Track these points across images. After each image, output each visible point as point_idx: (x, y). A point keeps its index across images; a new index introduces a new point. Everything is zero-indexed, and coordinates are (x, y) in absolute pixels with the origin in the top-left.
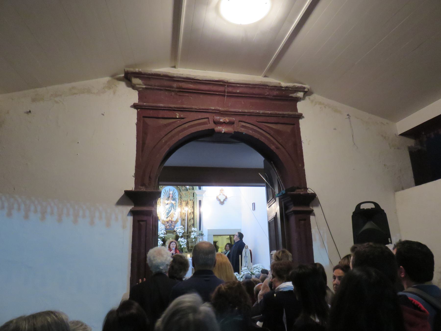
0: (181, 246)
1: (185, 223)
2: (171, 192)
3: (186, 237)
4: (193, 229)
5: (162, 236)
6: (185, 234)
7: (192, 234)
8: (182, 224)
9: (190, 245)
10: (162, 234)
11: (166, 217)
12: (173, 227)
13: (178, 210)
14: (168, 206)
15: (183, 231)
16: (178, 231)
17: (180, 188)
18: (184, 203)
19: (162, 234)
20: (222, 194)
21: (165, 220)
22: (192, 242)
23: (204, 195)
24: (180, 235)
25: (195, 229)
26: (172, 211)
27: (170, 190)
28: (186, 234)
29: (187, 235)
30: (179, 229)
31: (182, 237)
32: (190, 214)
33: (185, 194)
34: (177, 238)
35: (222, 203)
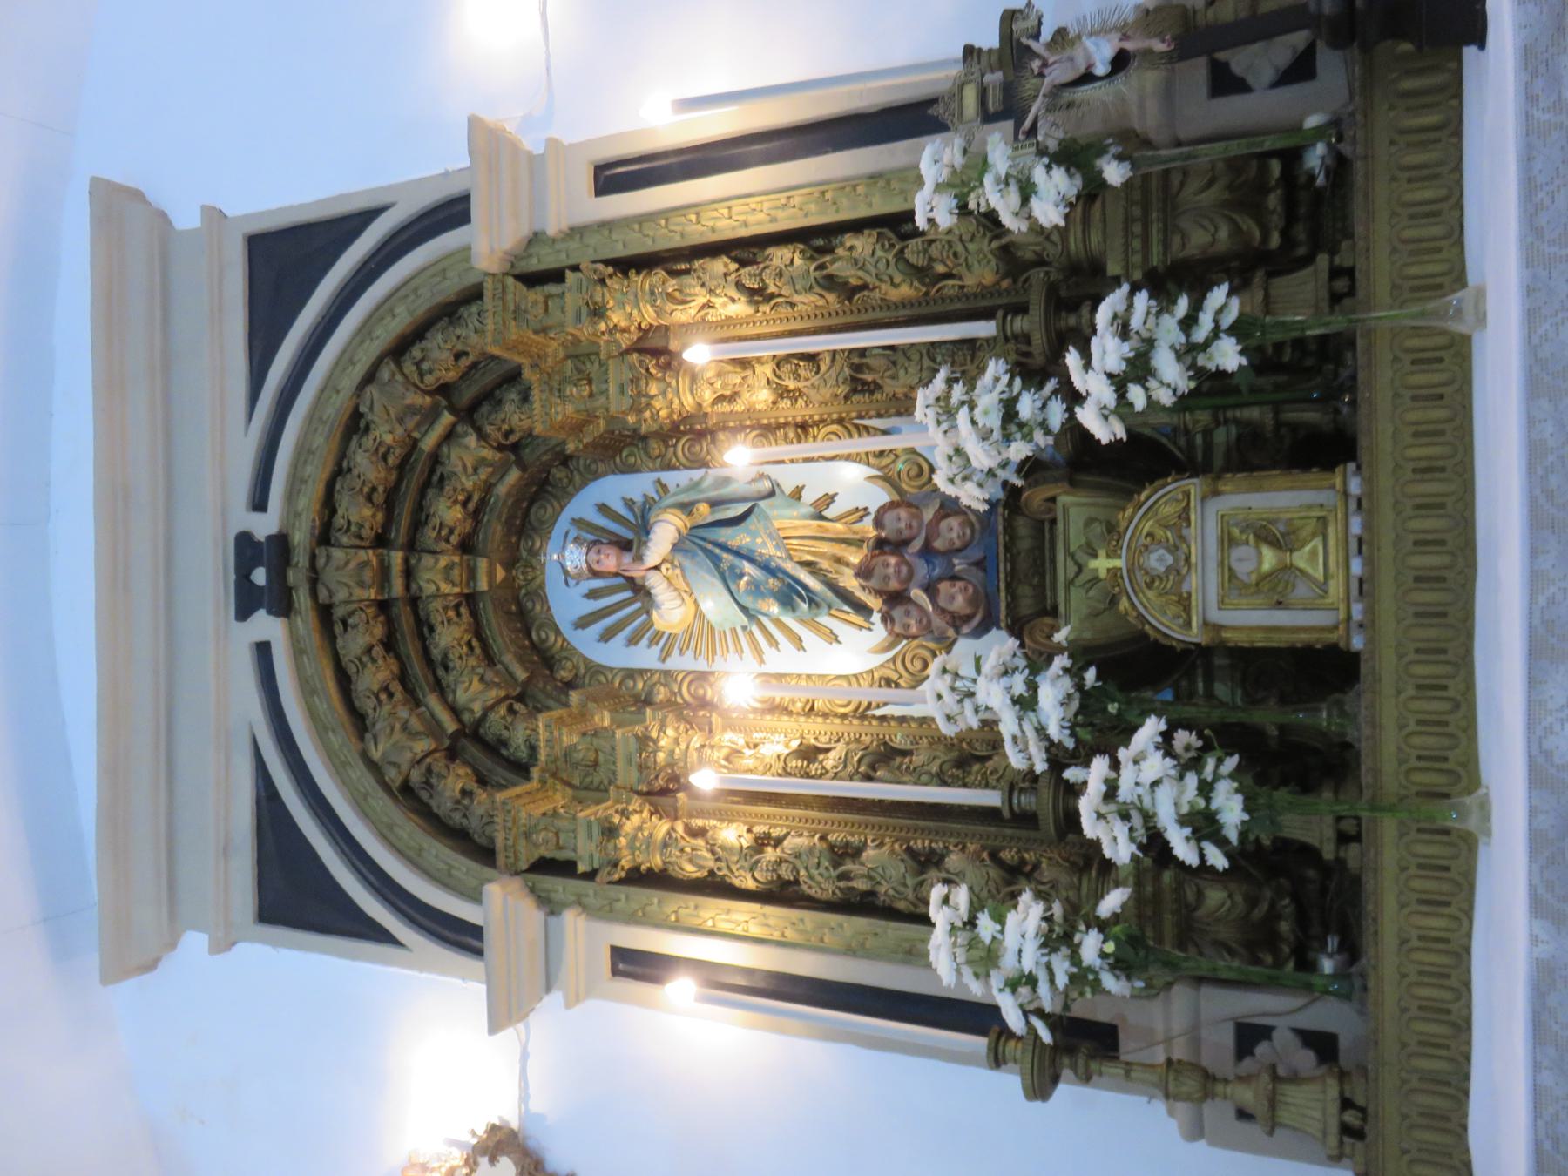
2: (575, 557)
5: (1053, 693)
7: (1003, 203)
8: (905, 407)
10: (1026, 703)
12: (952, 531)
15: (995, 367)
19: (1026, 703)
23: (532, 143)
26: (768, 550)
28: (1029, 323)
30: (964, 441)
32: (758, 295)
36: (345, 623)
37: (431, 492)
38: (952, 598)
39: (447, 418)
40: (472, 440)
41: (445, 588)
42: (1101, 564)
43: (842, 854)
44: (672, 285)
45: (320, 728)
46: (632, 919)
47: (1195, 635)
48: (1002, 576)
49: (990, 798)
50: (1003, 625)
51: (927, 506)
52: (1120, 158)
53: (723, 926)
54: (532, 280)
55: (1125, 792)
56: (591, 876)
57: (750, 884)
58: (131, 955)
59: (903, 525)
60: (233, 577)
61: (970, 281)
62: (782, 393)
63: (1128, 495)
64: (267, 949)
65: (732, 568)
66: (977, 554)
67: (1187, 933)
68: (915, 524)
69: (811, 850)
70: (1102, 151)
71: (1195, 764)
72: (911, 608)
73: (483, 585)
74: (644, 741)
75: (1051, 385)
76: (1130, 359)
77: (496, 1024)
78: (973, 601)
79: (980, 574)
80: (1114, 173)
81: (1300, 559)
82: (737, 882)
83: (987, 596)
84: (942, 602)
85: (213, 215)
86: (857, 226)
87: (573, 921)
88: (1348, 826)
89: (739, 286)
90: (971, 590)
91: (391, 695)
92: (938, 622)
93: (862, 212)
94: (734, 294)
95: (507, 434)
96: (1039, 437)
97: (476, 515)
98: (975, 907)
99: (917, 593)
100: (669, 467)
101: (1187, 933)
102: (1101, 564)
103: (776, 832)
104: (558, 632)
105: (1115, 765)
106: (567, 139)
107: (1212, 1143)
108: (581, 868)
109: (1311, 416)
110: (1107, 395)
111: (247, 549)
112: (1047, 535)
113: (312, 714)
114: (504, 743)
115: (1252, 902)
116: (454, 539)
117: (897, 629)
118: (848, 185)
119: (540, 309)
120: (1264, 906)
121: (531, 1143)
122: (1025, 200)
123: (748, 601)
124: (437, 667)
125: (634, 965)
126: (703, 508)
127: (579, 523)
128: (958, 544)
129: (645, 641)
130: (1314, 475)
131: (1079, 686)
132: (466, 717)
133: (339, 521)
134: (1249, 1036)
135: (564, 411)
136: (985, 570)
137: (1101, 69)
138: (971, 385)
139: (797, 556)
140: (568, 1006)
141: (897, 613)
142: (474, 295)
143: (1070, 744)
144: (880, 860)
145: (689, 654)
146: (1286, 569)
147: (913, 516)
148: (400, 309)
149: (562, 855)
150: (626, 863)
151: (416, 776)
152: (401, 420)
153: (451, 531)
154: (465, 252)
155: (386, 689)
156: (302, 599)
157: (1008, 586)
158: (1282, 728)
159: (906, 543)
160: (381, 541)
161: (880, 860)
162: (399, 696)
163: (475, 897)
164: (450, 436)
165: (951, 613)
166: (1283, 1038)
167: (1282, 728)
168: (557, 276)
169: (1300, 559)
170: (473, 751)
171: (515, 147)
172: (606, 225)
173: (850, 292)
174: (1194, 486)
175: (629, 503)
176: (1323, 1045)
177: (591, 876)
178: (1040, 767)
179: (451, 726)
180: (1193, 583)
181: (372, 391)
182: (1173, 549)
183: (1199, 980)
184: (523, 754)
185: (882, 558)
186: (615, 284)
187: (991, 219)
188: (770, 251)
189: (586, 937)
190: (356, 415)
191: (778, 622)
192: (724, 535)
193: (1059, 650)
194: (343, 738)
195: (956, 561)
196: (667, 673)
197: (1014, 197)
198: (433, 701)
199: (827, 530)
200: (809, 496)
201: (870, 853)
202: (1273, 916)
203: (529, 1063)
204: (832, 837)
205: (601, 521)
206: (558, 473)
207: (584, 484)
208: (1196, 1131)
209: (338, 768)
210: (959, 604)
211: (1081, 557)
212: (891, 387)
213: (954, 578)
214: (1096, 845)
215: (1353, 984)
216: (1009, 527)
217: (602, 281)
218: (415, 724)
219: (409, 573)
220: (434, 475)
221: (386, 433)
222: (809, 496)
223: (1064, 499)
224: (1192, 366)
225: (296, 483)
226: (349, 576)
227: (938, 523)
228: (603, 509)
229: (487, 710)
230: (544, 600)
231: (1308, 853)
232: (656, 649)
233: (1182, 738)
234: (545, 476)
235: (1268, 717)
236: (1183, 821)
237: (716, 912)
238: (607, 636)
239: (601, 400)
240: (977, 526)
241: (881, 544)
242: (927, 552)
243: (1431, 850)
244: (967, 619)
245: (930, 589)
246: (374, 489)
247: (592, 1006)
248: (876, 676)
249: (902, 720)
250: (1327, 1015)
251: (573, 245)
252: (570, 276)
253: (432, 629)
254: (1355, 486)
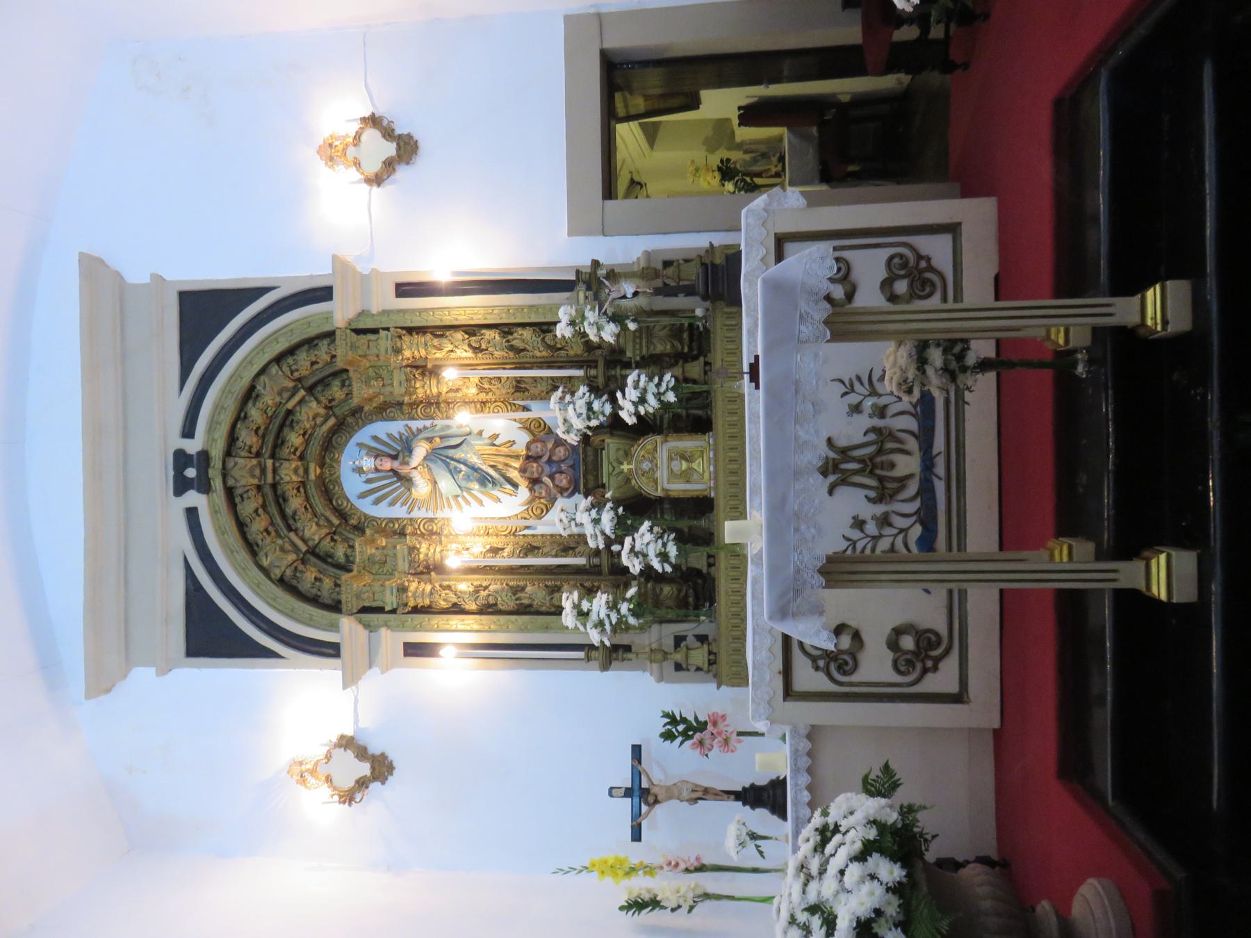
0: (665, 406)
1: (535, 380)
2: (368, 463)
3: (618, 371)
4: (563, 330)
5: (607, 518)
6: (601, 380)
9: (659, 348)
10: (596, 522)
11: (509, 487)
12: (561, 452)
13: (463, 419)
14: (446, 484)
15: (583, 389)
16: (579, 424)
17: (345, 409)
18: (425, 388)
19: (596, 522)
20: (352, 151)
21: (524, 493)
22: (645, 332)
23: (363, 268)
24: (602, 406)
25: (564, 314)
26: (474, 460)
27: (359, 470)
28: (599, 372)
29: (604, 368)
30: (569, 415)
31: (613, 400)
32: (477, 350)
33: (367, 382)
34: (615, 424)
35: (406, 148)
36: (241, 496)
37: (286, 430)
39: (302, 393)
40: (314, 404)
41: (295, 478)
42: (625, 467)
43: (516, 590)
44: (436, 342)
45: (229, 552)
46: (414, 629)
47: (659, 493)
49: (581, 561)
52: (634, 321)
53: (460, 627)
54: (358, 332)
55: (637, 549)
56: (394, 611)
57: (473, 607)
58: (101, 682)
60: (171, 473)
61: (571, 353)
62: (481, 389)
63: (636, 440)
64: (195, 670)
65: (455, 468)
66: (571, 462)
67: (657, 604)
69: (503, 589)
70: (627, 318)
71: (661, 537)
73: (312, 476)
74: (412, 549)
75: (605, 397)
76: (639, 394)
77: (345, 687)
78: (570, 482)
80: (632, 326)
81: (695, 465)
82: (467, 607)
85: (158, 279)
86: (523, 325)
87: (384, 632)
88: (711, 560)
89: (470, 345)
91: (269, 533)
92: (554, 491)
93: (526, 320)
94: (466, 348)
95: (330, 401)
96: (602, 418)
97: (307, 442)
98: (580, 599)
99: (546, 479)
100: (413, 419)
101: (657, 604)
102: (625, 467)
103: (485, 584)
104: (348, 501)
105: (634, 540)
106: (384, 268)
107: (667, 682)
108: (388, 608)
109: (699, 412)
110: (632, 409)
111: (181, 459)
113: (225, 546)
114: (331, 556)
115: (679, 591)
116: (298, 453)
118: (520, 309)
119: (365, 347)
120: (682, 594)
121: (361, 743)
122: (599, 330)
123: (463, 484)
124: (289, 522)
125: (414, 650)
126: (438, 440)
127: (360, 445)
129: (399, 504)
130: (699, 436)
131: (617, 514)
132: (310, 543)
133: (239, 444)
134: (679, 640)
135: (367, 392)
137: (629, 296)
138: (573, 394)
140: (383, 673)
141: (537, 487)
142: (330, 335)
143: (613, 537)
144: (534, 592)
145: (424, 510)
146: (690, 469)
148: (281, 340)
149: (374, 604)
150: (411, 604)
151: (289, 572)
152: (280, 394)
153: (296, 449)
154: (328, 317)
155: (267, 530)
156: (217, 483)
158: (690, 528)
159: (540, 457)
160: (258, 455)
161: (534, 592)
162: (273, 534)
163: (334, 627)
164: (301, 402)
166: (691, 640)
167: (690, 528)
168: (375, 331)
169: (695, 465)
170: (313, 559)
171: (354, 270)
172: (404, 311)
173: (518, 351)
174: (659, 438)
175: (389, 435)
176: (702, 639)
177: (394, 611)
178: (601, 546)
179: (304, 548)
180: (658, 474)
181: (262, 378)
182: (651, 461)
183: (661, 622)
184: (342, 560)
186: (407, 338)
187: (584, 335)
188: (483, 331)
189: (391, 639)
190: (252, 388)
192: (451, 452)
193: (608, 500)
194: (243, 556)
196: (411, 519)
197: (595, 330)
198: (292, 535)
200: (486, 435)
201: (529, 589)
202: (686, 596)
203: (359, 705)
204: (511, 584)
205: (374, 444)
206: (350, 420)
207: (364, 425)
208: (661, 679)
209: (241, 571)
210: (564, 483)
211: (615, 464)
212: (533, 391)
213: (561, 472)
214: (627, 568)
215: (712, 616)
216: (585, 451)
217: (400, 337)
218: (288, 547)
219: (275, 471)
220: (288, 419)
221: (268, 398)
222: (486, 435)
223: (608, 441)
224: (659, 400)
225: (212, 425)
226: (244, 472)
228: (375, 438)
229: (320, 540)
230: (340, 485)
231: (698, 572)
232: (405, 508)
233: (656, 529)
234: (345, 423)
235: (684, 524)
236: (657, 556)
237: (455, 621)
238: (377, 502)
239: (389, 389)
241: (528, 457)
242: (550, 461)
243: (734, 562)
245: (552, 477)
246: (258, 428)
247: (395, 672)
249: (533, 536)
250: (705, 627)
251: (384, 319)
252: (382, 333)
253: (285, 500)
254: (711, 441)
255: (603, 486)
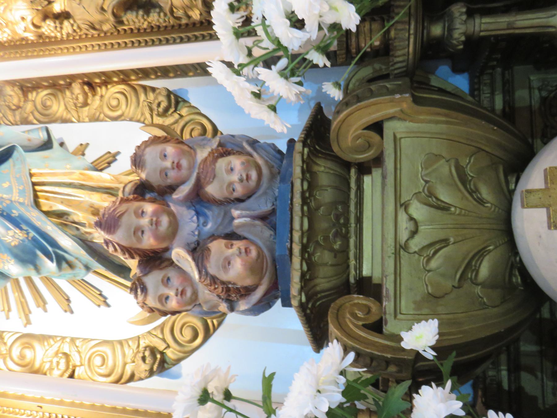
38: (228, 262)
48: (296, 236)
50: (295, 302)
51: (203, 146)
59: (168, 164)
66: (263, 206)
68: (184, 163)
72: (171, 273)
78: (256, 268)
79: (268, 233)
83: (274, 260)
84: (212, 268)
90: (254, 253)
92: (206, 294)
112: (353, 185)
117: (151, 302)
128: (239, 191)
136: (273, 228)
139: (46, 205)
141: (153, 280)
147: (182, 153)
157: (304, 249)
159: (172, 188)
165: (223, 283)
185: (136, 204)
191: (48, 281)
195: (236, 213)
199: (91, 179)
210: (237, 272)
213: (231, 236)
216: (308, 171)
222: (92, 155)
227: (215, 159)
240: (265, 171)
241: (142, 190)
244: (247, 291)
248: (143, 344)
255: (369, 288)
